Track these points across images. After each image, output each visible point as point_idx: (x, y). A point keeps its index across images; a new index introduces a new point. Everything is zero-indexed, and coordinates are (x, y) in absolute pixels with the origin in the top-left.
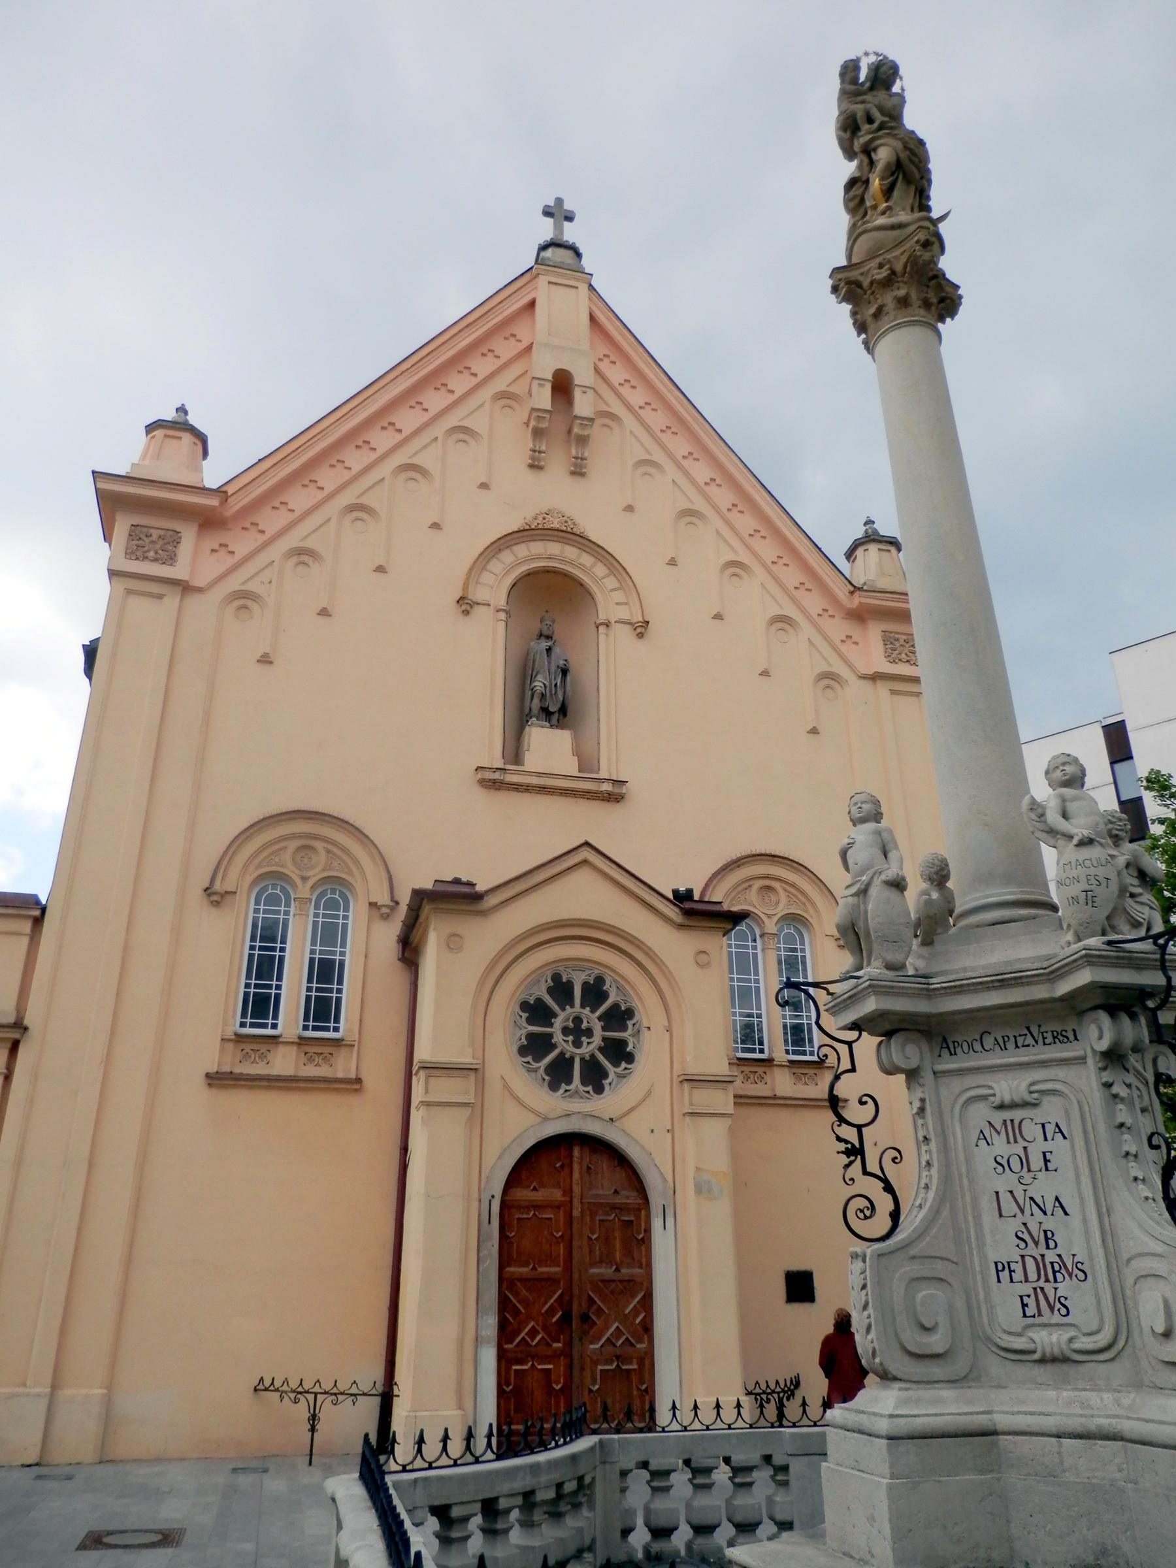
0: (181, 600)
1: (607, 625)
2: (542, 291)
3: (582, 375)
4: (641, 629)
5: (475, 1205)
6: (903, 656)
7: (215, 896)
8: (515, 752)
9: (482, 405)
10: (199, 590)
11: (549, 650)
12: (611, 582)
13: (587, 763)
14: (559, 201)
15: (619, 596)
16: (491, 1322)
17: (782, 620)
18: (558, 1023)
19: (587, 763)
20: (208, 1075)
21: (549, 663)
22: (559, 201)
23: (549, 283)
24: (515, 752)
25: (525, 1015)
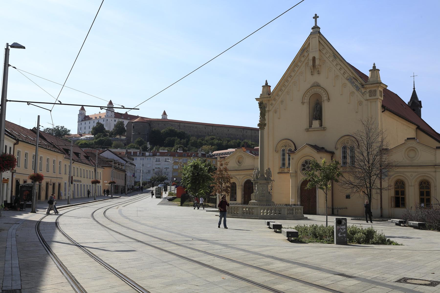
0: (268, 113)
1: (324, 101)
2: (311, 40)
3: (317, 57)
4: (329, 99)
5: (297, 188)
6: (373, 95)
7: (276, 151)
8: (310, 126)
9: (304, 66)
10: (270, 110)
11: (316, 107)
12: (324, 93)
13: (321, 125)
14: (316, 15)
15: (325, 96)
16: (299, 199)
17: (353, 92)
18: (306, 167)
19: (321, 125)
20: (278, 173)
21: (316, 109)
22: (316, 15)
23: (312, 38)
24: (310, 126)
25: (302, 166)
